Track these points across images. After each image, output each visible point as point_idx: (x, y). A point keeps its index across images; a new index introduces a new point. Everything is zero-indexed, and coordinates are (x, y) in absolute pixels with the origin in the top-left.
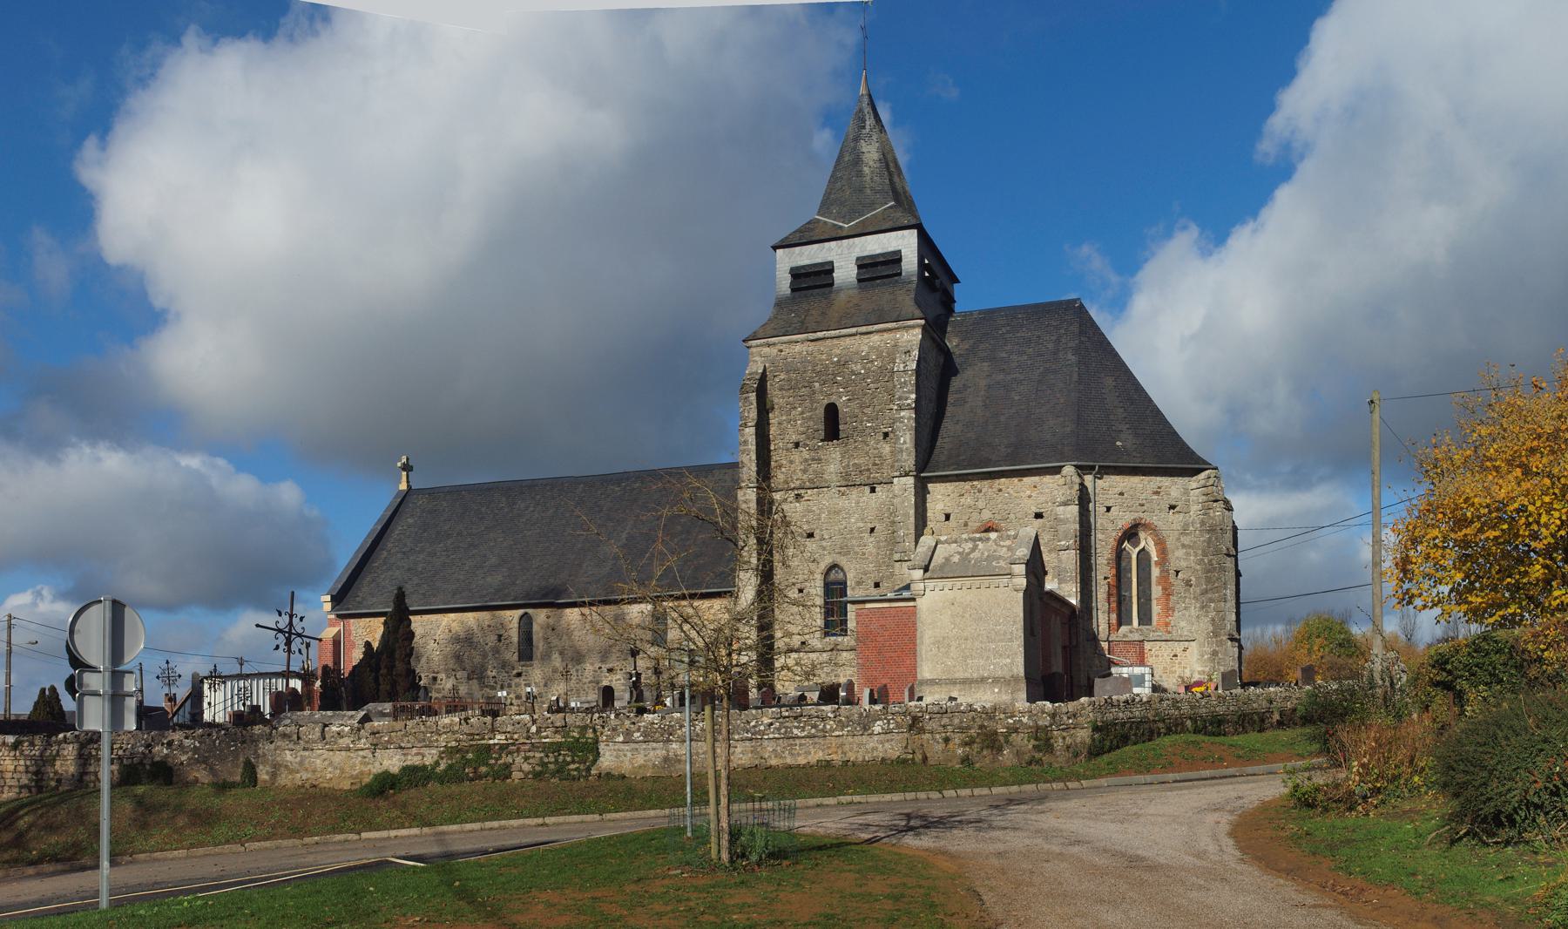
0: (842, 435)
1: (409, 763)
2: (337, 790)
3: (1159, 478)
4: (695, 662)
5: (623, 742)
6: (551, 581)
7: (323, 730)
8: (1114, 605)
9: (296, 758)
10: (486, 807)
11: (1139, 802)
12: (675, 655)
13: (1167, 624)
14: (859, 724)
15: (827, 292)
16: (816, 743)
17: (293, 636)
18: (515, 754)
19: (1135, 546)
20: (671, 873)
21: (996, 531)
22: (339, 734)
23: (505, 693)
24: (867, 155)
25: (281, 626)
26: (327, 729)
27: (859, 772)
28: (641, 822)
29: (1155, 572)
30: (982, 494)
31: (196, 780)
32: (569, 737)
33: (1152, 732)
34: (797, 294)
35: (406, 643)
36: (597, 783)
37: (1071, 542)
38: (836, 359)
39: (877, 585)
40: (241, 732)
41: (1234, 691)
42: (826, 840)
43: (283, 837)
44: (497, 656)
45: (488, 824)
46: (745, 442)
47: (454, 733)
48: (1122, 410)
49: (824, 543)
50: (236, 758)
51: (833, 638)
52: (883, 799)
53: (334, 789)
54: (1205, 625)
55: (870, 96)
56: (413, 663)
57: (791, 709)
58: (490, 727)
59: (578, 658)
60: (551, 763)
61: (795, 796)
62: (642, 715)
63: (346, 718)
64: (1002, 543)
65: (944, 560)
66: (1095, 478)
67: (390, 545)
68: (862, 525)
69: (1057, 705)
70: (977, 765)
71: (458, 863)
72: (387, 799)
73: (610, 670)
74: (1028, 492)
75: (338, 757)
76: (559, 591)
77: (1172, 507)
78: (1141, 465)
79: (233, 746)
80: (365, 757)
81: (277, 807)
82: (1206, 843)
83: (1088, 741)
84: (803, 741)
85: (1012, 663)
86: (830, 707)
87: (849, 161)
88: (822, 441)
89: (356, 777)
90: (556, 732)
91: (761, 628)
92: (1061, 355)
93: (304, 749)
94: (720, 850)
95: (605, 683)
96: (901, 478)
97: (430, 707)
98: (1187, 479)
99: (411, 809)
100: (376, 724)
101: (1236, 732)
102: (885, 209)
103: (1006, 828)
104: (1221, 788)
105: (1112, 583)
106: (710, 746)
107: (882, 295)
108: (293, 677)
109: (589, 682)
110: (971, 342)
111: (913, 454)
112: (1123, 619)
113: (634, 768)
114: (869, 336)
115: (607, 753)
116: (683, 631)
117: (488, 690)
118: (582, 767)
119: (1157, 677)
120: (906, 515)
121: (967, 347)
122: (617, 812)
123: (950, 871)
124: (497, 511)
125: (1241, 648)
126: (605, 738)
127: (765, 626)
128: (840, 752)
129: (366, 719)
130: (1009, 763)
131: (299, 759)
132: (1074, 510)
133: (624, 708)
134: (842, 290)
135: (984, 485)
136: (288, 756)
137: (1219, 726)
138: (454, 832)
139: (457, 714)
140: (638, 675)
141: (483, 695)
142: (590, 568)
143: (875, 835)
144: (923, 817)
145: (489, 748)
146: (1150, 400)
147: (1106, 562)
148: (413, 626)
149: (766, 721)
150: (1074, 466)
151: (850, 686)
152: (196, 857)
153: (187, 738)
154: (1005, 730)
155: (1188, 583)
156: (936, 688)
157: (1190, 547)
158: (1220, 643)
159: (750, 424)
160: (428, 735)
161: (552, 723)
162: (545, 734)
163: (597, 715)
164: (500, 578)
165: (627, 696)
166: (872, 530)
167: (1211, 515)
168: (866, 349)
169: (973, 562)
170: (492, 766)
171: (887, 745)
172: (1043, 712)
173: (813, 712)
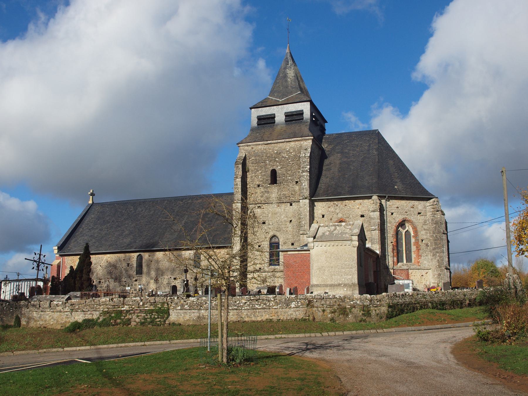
1: (86, 318)
2: (55, 329)
6: (151, 241)
7: (50, 303)
8: (395, 254)
11: (410, 338)
12: (205, 272)
13: (418, 262)
14: (285, 303)
16: (265, 312)
17: (40, 263)
18: (133, 314)
19: (404, 229)
20: (200, 367)
21: (344, 222)
22: (57, 305)
23: (129, 288)
24: (289, 74)
25: (35, 259)
26: (52, 303)
27: (285, 324)
28: (187, 344)
29: (413, 240)
30: (338, 207)
32: (157, 307)
33: (414, 308)
34: (260, 126)
37: (377, 227)
38: (276, 152)
39: (293, 244)
40: (15, 304)
41: (449, 291)
42: (270, 354)
43: (30, 349)
45: (120, 345)
46: (237, 184)
47: (106, 305)
48: (397, 174)
49: (270, 226)
50: (13, 315)
51: (273, 267)
53: (53, 328)
54: (435, 263)
55: (290, 53)
56: (91, 276)
58: (122, 302)
60: (148, 318)
61: (256, 335)
62: (189, 298)
63: (60, 298)
64: (347, 227)
66: (386, 201)
67: (83, 226)
68: (286, 219)
69: (372, 296)
70: (337, 322)
72: (76, 333)
73: (175, 279)
74: (358, 206)
75: (56, 315)
77: (419, 213)
78: (405, 196)
79: (11, 310)
80: (68, 315)
82: (441, 356)
83: (386, 312)
84: (260, 310)
85: (352, 278)
86: (272, 295)
88: (269, 184)
90: (151, 305)
91: (242, 262)
93: (42, 311)
95: (173, 284)
96: (303, 200)
97: (97, 294)
98: (425, 202)
99: (86, 338)
100: (73, 301)
101: (451, 309)
102: (297, 94)
103: (350, 349)
104: (446, 333)
105: (394, 245)
106: (219, 311)
107: (295, 127)
108: (39, 281)
110: (333, 146)
112: (399, 260)
113: (185, 321)
115: (173, 314)
116: (209, 261)
119: (415, 285)
120: (305, 215)
121: (331, 147)
122: (177, 340)
123: (326, 368)
125: (450, 272)
126: (172, 307)
127: (244, 260)
128: (276, 316)
129: (69, 298)
130: (351, 321)
131: (39, 315)
132: (377, 214)
135: (340, 203)
136: (35, 314)
137: (443, 306)
138: (105, 348)
139: (108, 297)
140: (187, 281)
143: (292, 352)
144: (313, 344)
146: (409, 170)
147: (392, 236)
148: (92, 260)
149: (244, 301)
151: (281, 287)
154: (349, 307)
155: (427, 245)
156: (319, 288)
157: (427, 230)
158: (442, 270)
160: (96, 306)
161: (149, 301)
162: (146, 306)
165: (182, 290)
166: (291, 221)
168: (288, 148)
169: (335, 235)
171: (297, 313)
172: (366, 299)
173: (264, 298)
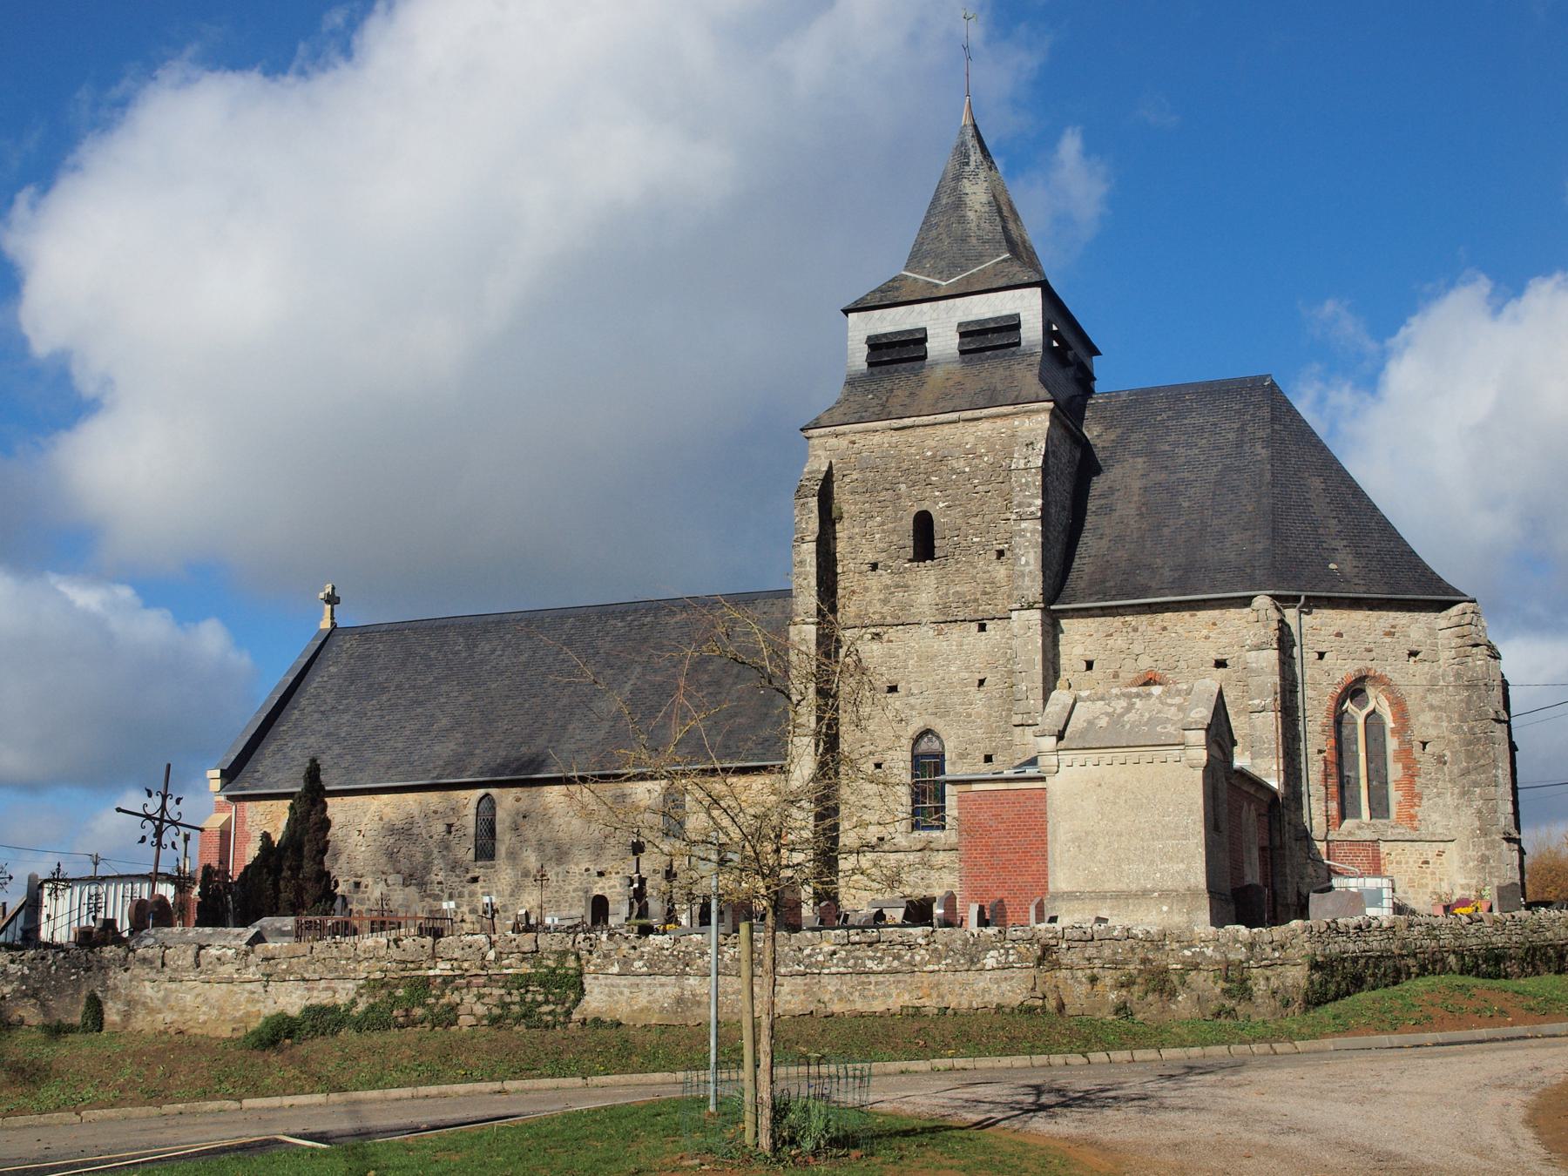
0: (937, 553)
1: (314, 1001)
2: (212, 1039)
3: (1392, 614)
4: (726, 862)
5: (618, 975)
6: (524, 749)
7: (198, 955)
8: (1333, 789)
9: (158, 992)
10: (420, 1066)
12: (699, 851)
13: (1412, 817)
14: (963, 955)
15: (917, 367)
16: (899, 982)
17: (166, 825)
18: (465, 991)
19: (1362, 706)
20: (685, 1163)
21: (1160, 684)
22: (219, 959)
23: (452, 904)
25: (150, 810)
26: (203, 952)
27: (963, 1024)
28: (641, 1089)
29: (1392, 744)
30: (1138, 634)
31: (22, 1021)
33: (1398, 971)
34: (876, 370)
35: (320, 835)
36: (580, 1033)
38: (929, 454)
39: (988, 759)
40: (86, 955)
41: (1516, 913)
43: (133, 1103)
44: (445, 853)
45: (423, 1090)
47: (379, 959)
48: (1335, 522)
49: (912, 700)
50: (78, 991)
51: (924, 834)
52: (1000, 1065)
53: (208, 1037)
54: (1467, 819)
55: (975, 126)
56: (327, 864)
57: (864, 932)
58: (430, 951)
59: (561, 854)
60: (514, 1004)
62: (647, 936)
63: (230, 938)
64: (1169, 701)
65: (1085, 724)
66: (1301, 612)
67: (304, 702)
68: (967, 675)
69: (1255, 930)
70: (1139, 1017)
71: (374, 1144)
72: (281, 1051)
73: (601, 874)
74: (1205, 632)
75: (217, 992)
76: (537, 763)
77: (1413, 654)
78: (1365, 595)
79: (73, 974)
80: (254, 992)
81: (129, 1061)
82: (1489, 1133)
83: (1304, 983)
84: (880, 978)
85: (1188, 870)
86: (921, 928)
87: (947, 203)
88: (910, 561)
89: (241, 1020)
90: (523, 960)
91: (819, 817)
92: (1246, 447)
93: (171, 980)
94: (757, 1132)
95: (597, 891)
96: (1023, 612)
97: (347, 923)
98: (1433, 615)
99: (315, 1067)
100: (271, 945)
101: (1523, 974)
102: (997, 263)
103: (1184, 1109)
104: (1508, 1054)
105: (1329, 758)
107: (993, 372)
108: (162, 881)
109: (574, 891)
110: (1119, 431)
111: (1040, 578)
112: (1346, 810)
113: (633, 1011)
114: (975, 423)
115: (596, 990)
116: (710, 815)
117: (431, 901)
118: (559, 1009)
119: (1399, 893)
120: (1031, 662)
121: (1113, 437)
122: (608, 1074)
123: (1102, 1171)
124: (450, 656)
125: (1522, 852)
126: (592, 968)
127: (827, 811)
128: (934, 995)
129: (258, 938)
130: (1186, 1014)
131: (162, 993)
132: (1272, 656)
133: (621, 926)
134: (937, 364)
136: (148, 990)
137: (1497, 964)
138: (373, 1101)
139: (384, 933)
140: (642, 881)
141: (424, 907)
142: (578, 731)
143: (988, 1115)
145: (427, 982)
146: (1375, 508)
148: (329, 813)
149: (827, 948)
150: (1270, 596)
151: (950, 900)
152: (13, 1129)
153: (12, 962)
154: (1179, 966)
155: (1441, 760)
156: (1076, 904)
157: (1441, 709)
158: (1492, 845)
159: (808, 539)
160: (343, 962)
161: (518, 946)
162: (507, 962)
163: (581, 936)
164: (452, 746)
165: (625, 910)
166: (981, 682)
167: (1470, 664)
168: (971, 440)
169: (1128, 726)
170: (430, 1008)
171: (1005, 986)
172: (1236, 941)
173: (895, 937)
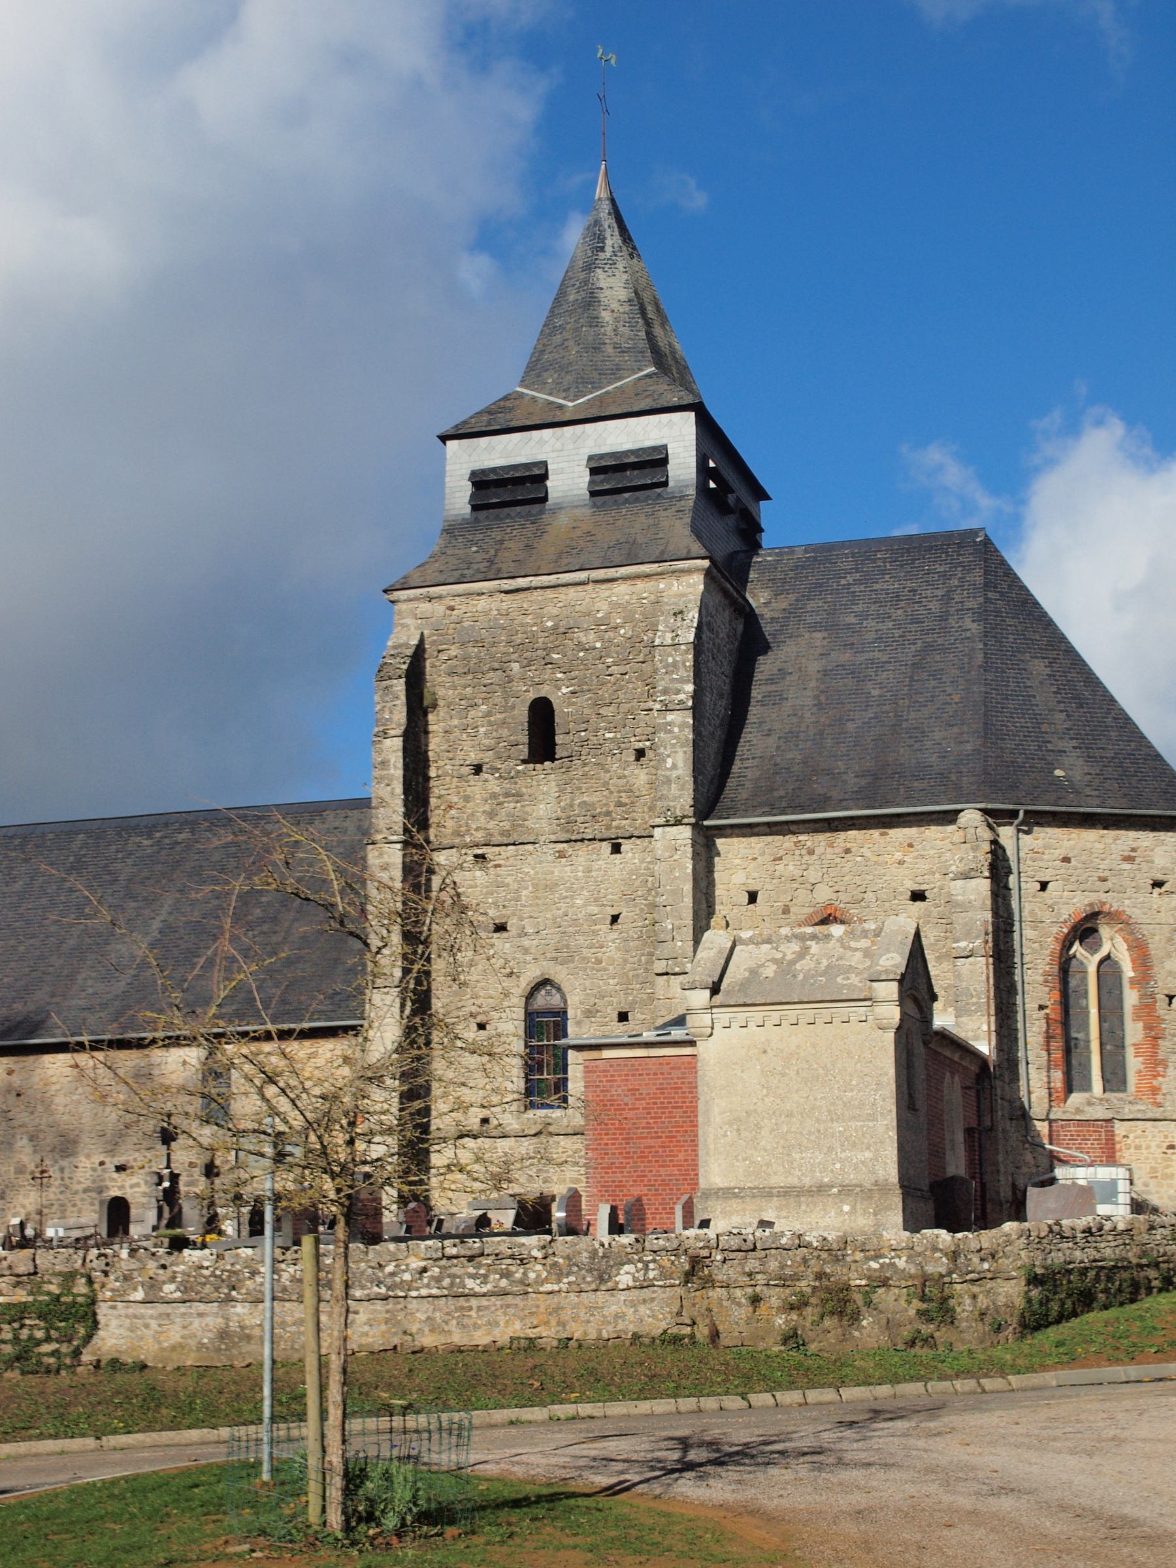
3: (1132, 834)
4: (284, 1156)
6: (18, 1006)
8: (1058, 1055)
11: (1120, 1416)
12: (248, 1143)
13: (1155, 1090)
14: (590, 1271)
16: (508, 1306)
19: (1093, 950)
20: (231, 1549)
21: (842, 922)
24: (608, 293)
27: (590, 1360)
28: (172, 1452)
29: (1131, 998)
30: (815, 857)
32: (42, 1294)
34: (482, 514)
36: (92, 1380)
37: (978, 942)
38: (550, 624)
39: (623, 1017)
42: (528, 1487)
46: (384, 764)
48: (1063, 716)
49: (526, 942)
55: (613, 201)
57: (463, 1242)
59: (67, 1146)
61: (468, 1406)
62: (180, 1250)
64: (853, 944)
66: (1019, 831)
69: (959, 1235)
70: (813, 1347)
73: (120, 1168)
74: (898, 856)
76: (34, 1025)
77: (1158, 884)
78: (1099, 810)
83: (1020, 1302)
84: (484, 1302)
86: (535, 1237)
88: (524, 762)
90: (17, 1284)
91: (408, 1096)
92: (952, 621)
96: (668, 829)
102: (639, 379)
103: (869, 1465)
105: (1052, 1016)
106: (311, 1311)
110: (792, 597)
111: (690, 786)
113: (162, 1349)
114: (609, 585)
115: (114, 1323)
116: (263, 1098)
118: (65, 1348)
121: (784, 605)
122: (129, 1432)
123: (766, 1547)
126: (109, 1294)
128: (553, 1322)
130: (872, 1343)
132: (982, 886)
135: (820, 840)
140: (174, 1178)
143: (622, 1478)
144: (712, 1445)
146: (1112, 700)
147: (1041, 979)
149: (416, 1264)
150: (980, 810)
151: (573, 1200)
154: (863, 1282)
156: (735, 1204)
159: (392, 733)
161: (10, 1267)
163: (94, 1252)
165: (151, 1217)
166: (615, 919)
169: (801, 977)
171: (643, 1310)
172: (935, 1249)
